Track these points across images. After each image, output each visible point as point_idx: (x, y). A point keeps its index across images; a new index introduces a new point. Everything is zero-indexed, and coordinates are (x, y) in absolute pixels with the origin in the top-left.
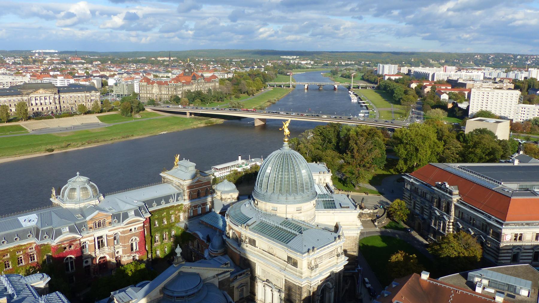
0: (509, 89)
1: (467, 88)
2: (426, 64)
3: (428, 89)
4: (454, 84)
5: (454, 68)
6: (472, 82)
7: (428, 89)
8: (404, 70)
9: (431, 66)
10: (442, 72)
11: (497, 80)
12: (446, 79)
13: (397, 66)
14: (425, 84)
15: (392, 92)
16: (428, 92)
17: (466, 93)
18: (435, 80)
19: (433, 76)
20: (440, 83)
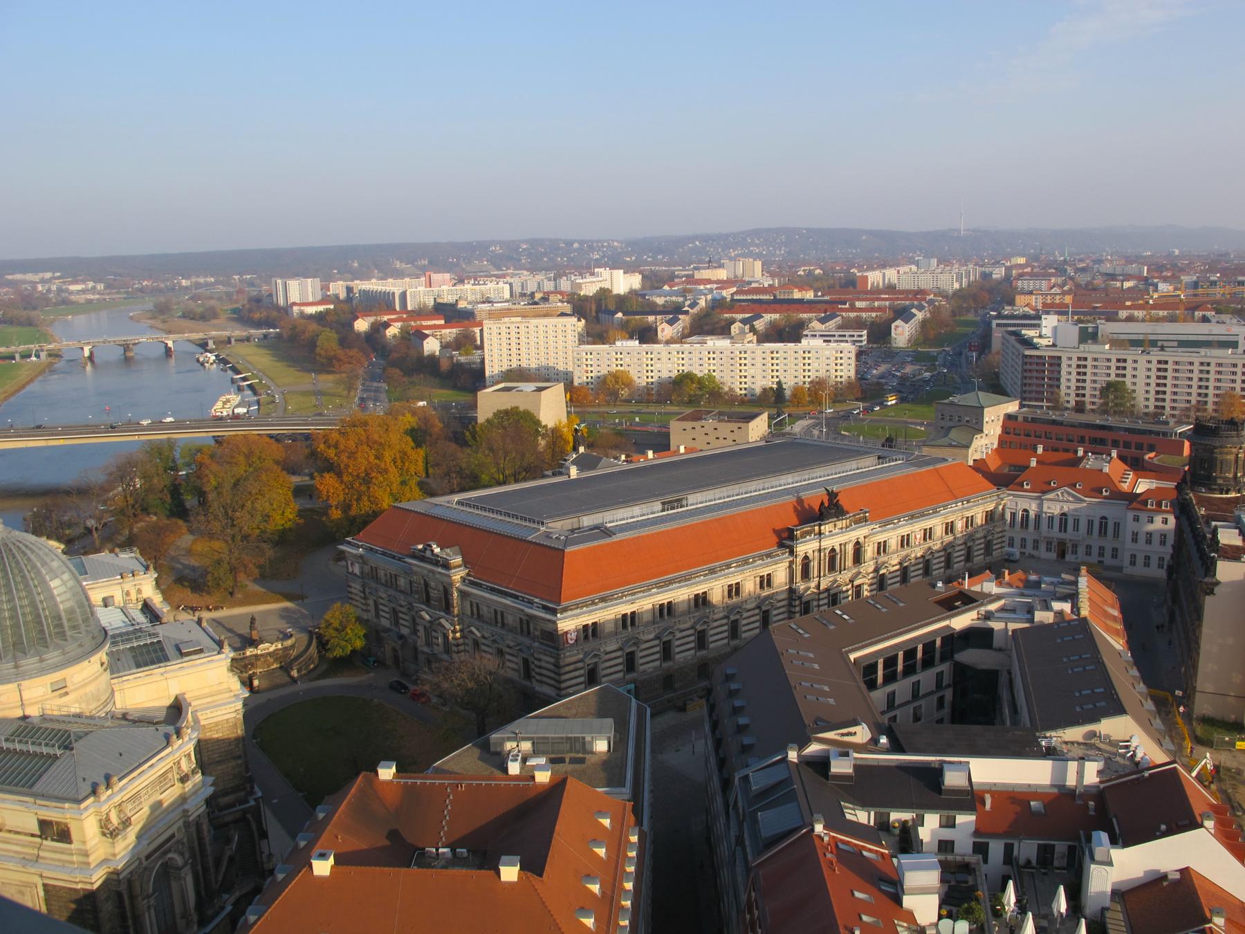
0: (563, 315)
1: (478, 319)
2: (389, 273)
3: (393, 331)
4: (449, 312)
5: (447, 276)
6: (486, 306)
7: (393, 331)
8: (338, 288)
9: (398, 274)
10: (421, 289)
11: (538, 296)
12: (432, 303)
13: (318, 280)
14: (385, 318)
15: (312, 344)
16: (394, 336)
17: (477, 330)
18: (409, 308)
19: (403, 296)
20: (420, 313)
